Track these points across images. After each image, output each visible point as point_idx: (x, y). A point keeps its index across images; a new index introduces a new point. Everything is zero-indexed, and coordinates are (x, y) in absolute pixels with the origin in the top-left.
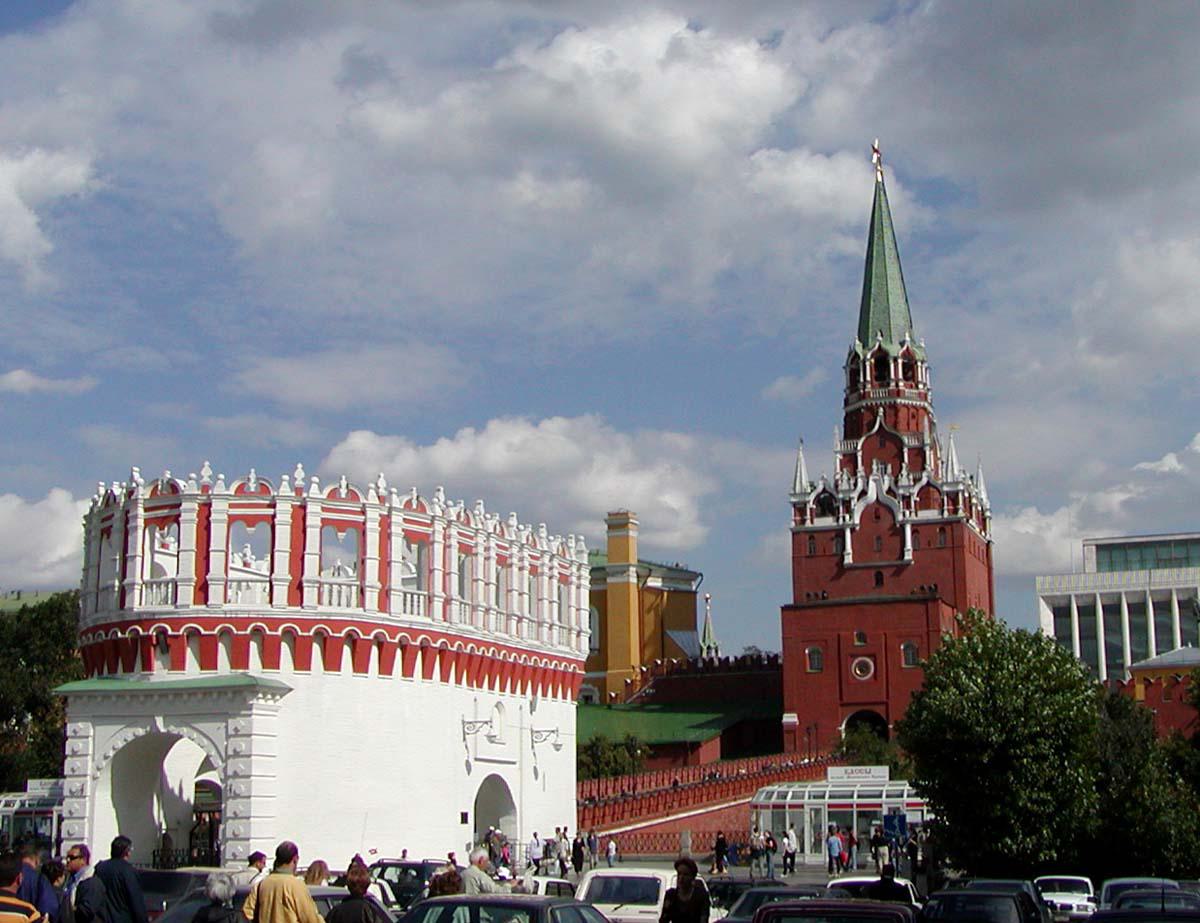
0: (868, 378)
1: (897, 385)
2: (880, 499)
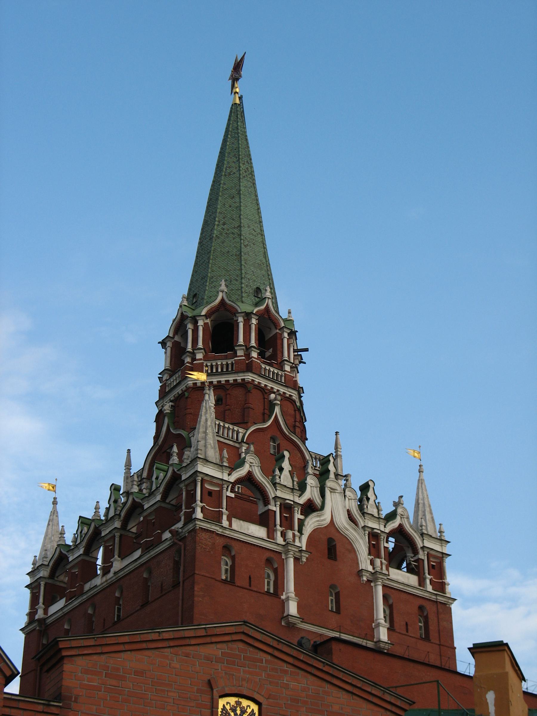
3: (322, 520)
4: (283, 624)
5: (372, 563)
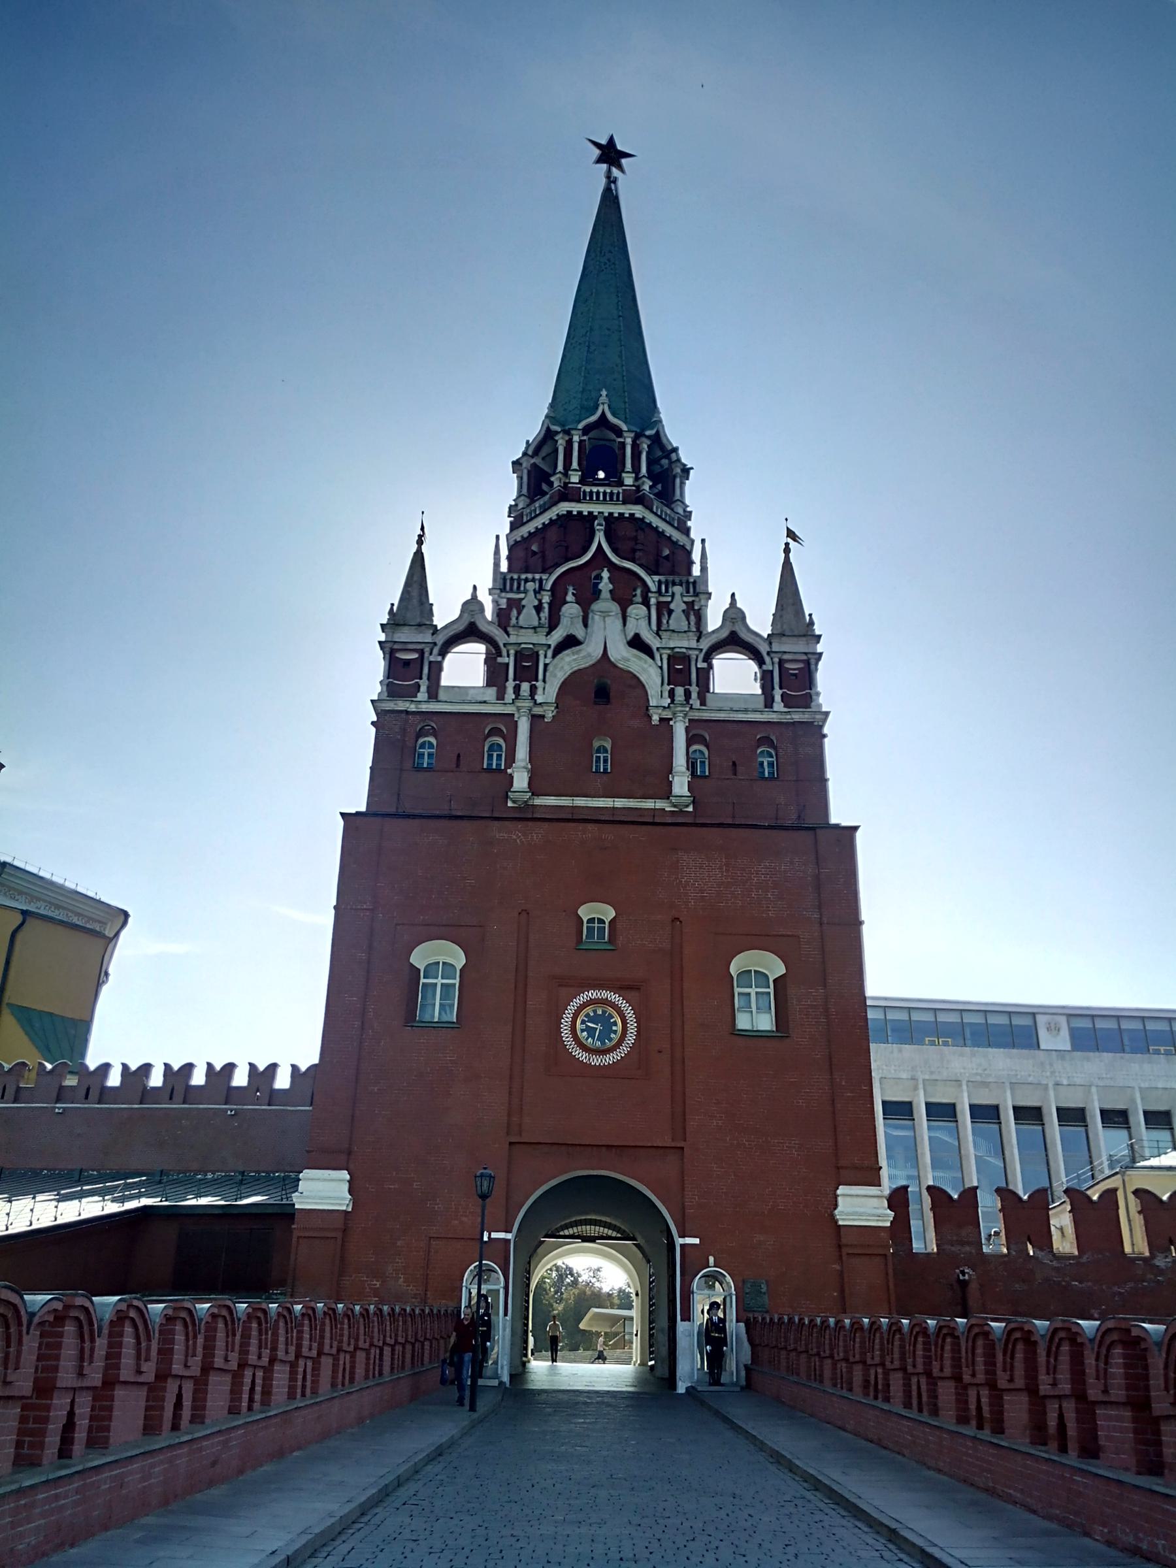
0: (575, 465)
1: (638, 487)
2: (613, 655)
3: (584, 657)
4: (510, 804)
5: (672, 694)
